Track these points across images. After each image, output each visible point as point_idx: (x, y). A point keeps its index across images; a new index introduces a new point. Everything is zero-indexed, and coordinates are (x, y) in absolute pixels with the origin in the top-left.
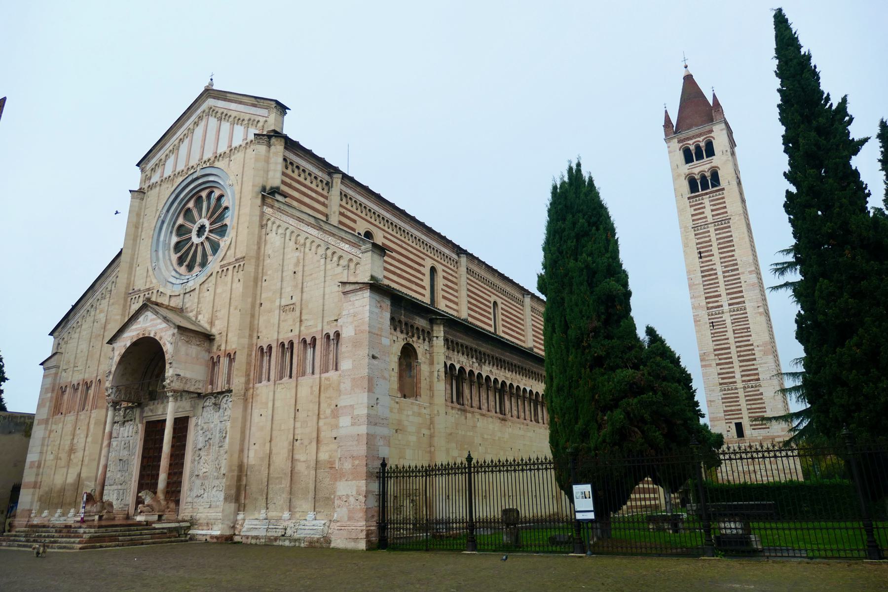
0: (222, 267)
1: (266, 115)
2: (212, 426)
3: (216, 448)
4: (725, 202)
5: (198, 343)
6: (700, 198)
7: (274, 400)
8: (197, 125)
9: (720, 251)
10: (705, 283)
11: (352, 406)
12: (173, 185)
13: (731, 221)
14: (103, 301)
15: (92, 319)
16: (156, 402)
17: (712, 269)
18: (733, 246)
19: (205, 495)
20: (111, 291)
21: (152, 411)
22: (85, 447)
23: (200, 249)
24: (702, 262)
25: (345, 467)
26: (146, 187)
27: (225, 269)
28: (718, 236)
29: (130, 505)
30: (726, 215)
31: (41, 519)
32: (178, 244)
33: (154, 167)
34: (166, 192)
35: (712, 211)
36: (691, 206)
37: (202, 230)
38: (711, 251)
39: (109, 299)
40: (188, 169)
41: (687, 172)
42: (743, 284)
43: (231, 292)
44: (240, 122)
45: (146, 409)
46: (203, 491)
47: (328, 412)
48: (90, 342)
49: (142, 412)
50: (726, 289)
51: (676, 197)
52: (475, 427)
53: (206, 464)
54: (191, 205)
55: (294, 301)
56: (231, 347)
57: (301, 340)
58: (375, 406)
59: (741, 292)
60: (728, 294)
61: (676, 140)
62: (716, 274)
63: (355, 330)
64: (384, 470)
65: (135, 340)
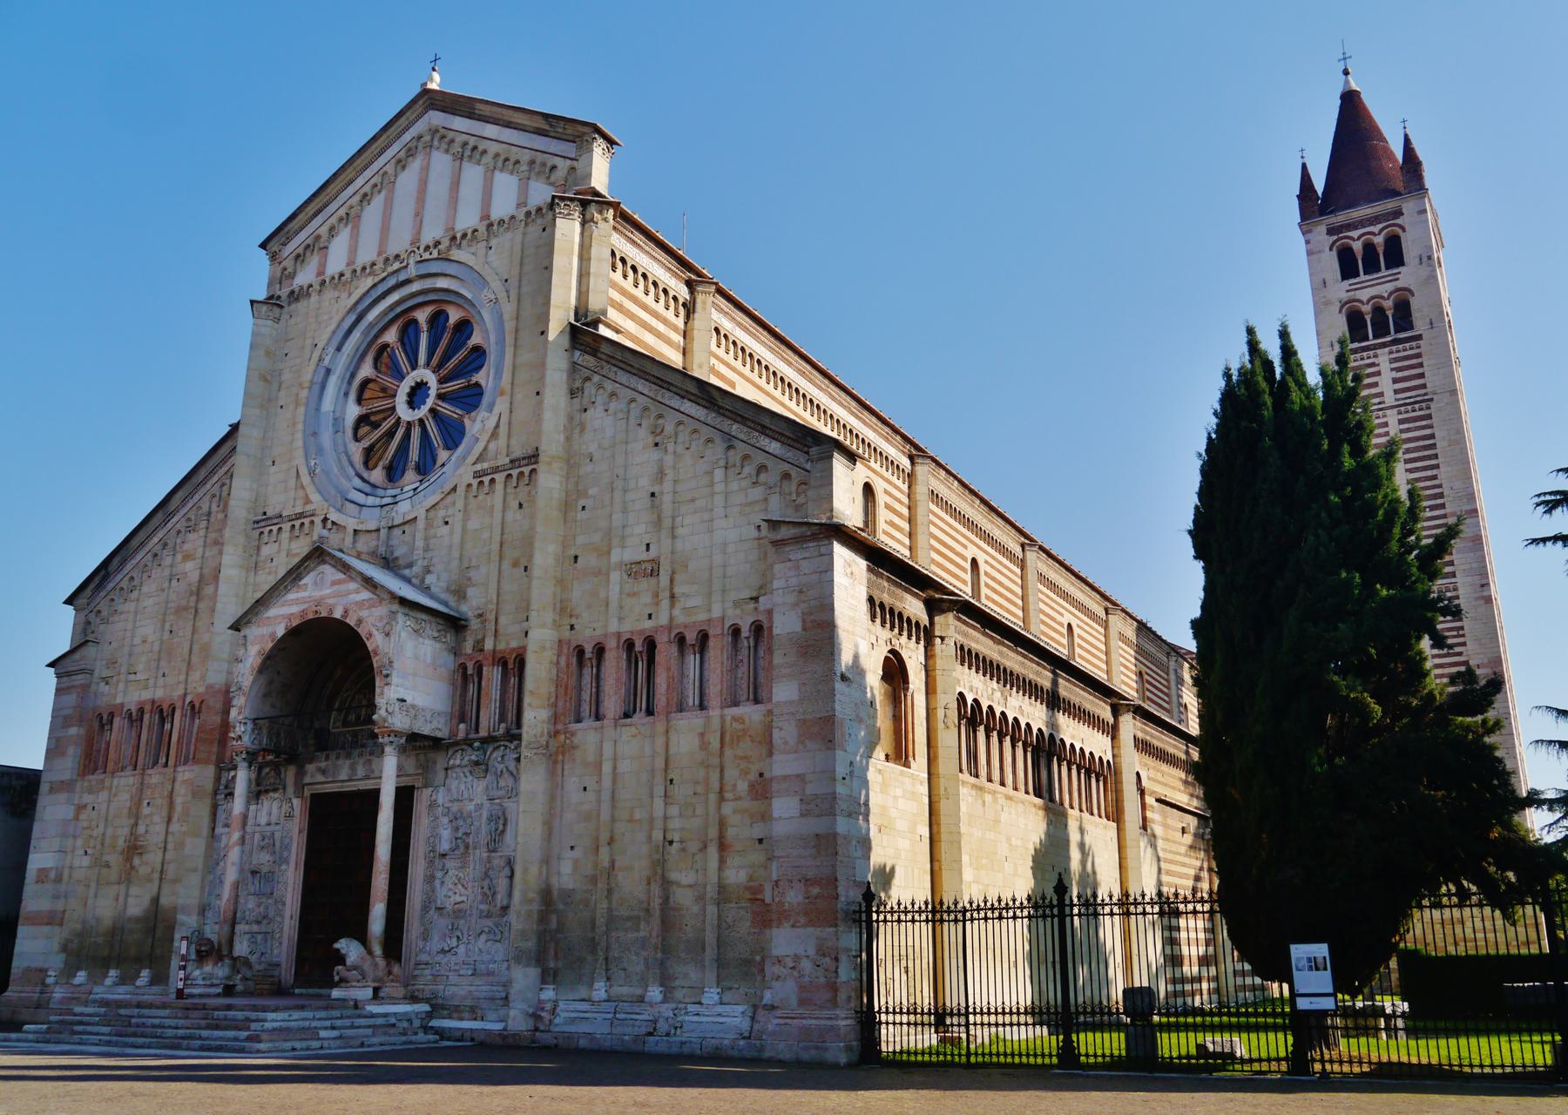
0: (477, 475)
1: (573, 156)
2: (471, 807)
3: (482, 853)
4: (1421, 365)
5: (436, 634)
6: (1371, 353)
7: (615, 760)
8: (404, 167)
11: (800, 777)
12: (350, 294)
13: (1433, 405)
14: (191, 536)
15: (167, 572)
16: (333, 755)
18: (1436, 456)
19: (462, 949)
20: (209, 513)
21: (324, 772)
22: (166, 842)
23: (416, 433)
25: (788, 899)
26: (284, 293)
27: (486, 479)
29: (283, 966)
30: (1423, 391)
31: (72, 990)
32: (362, 420)
33: (300, 250)
34: (332, 309)
35: (1395, 381)
37: (418, 392)
39: (207, 532)
40: (387, 259)
41: (1345, 296)
43: (502, 529)
44: (510, 165)
45: (310, 768)
46: (455, 940)
47: (743, 786)
48: (164, 621)
49: (301, 773)
51: (1319, 348)
52: (997, 822)
53: (460, 886)
54: (391, 336)
56: (508, 643)
57: (673, 635)
58: (848, 778)
61: (1323, 229)
63: (804, 621)
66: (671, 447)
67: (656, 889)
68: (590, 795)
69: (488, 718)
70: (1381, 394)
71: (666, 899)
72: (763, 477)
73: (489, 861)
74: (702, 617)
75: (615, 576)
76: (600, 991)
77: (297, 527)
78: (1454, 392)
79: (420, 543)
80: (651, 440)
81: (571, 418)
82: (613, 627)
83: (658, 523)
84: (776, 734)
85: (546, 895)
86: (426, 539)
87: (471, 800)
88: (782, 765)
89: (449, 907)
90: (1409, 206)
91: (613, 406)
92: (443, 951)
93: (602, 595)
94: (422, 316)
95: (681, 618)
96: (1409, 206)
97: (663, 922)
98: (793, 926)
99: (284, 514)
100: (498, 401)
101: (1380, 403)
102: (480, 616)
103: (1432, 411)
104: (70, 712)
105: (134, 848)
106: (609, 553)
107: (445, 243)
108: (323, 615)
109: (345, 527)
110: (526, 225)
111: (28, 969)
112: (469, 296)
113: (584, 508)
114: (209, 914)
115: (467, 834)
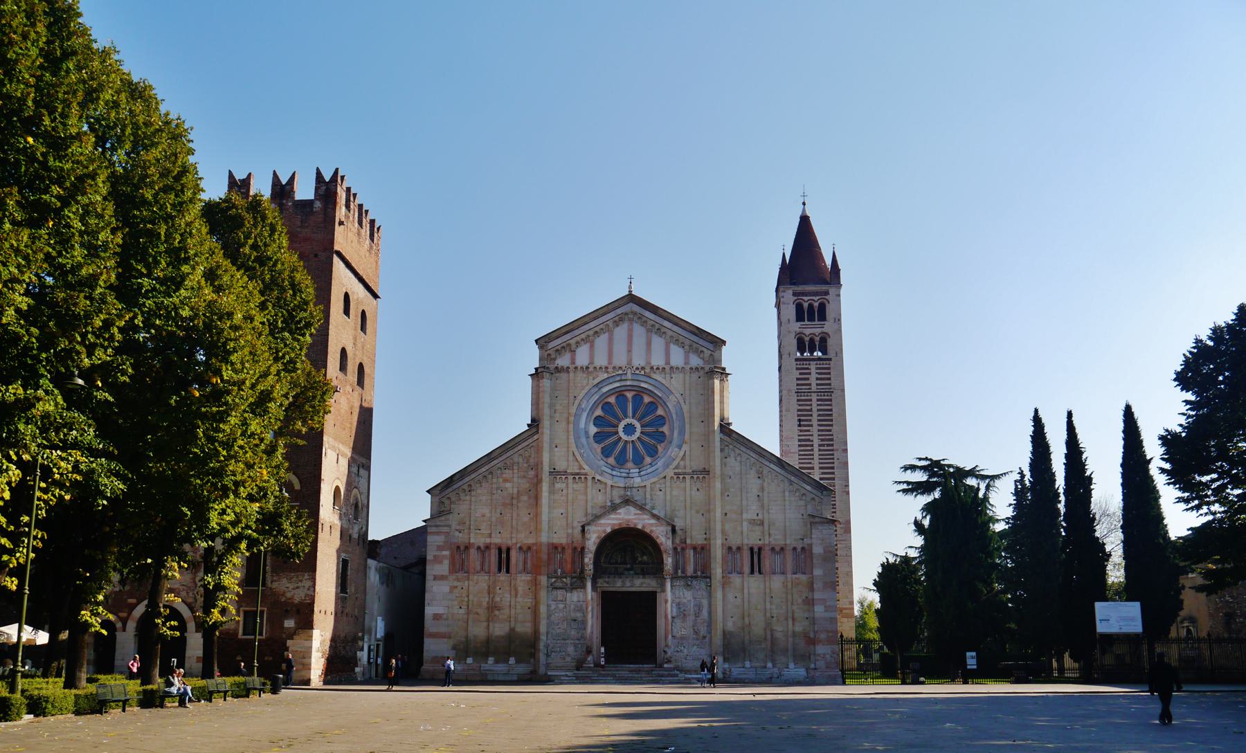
0: (675, 474)
3: (692, 618)
4: (829, 374)
6: (808, 362)
8: (617, 326)
9: (819, 423)
10: (801, 453)
11: (824, 600)
14: (507, 471)
17: (809, 440)
18: (832, 420)
19: (685, 651)
20: (518, 463)
21: (608, 583)
24: (801, 431)
26: (552, 367)
28: (819, 408)
35: (817, 379)
36: (797, 369)
38: (810, 420)
41: (798, 330)
42: (835, 461)
47: (800, 601)
50: (820, 463)
55: (760, 517)
59: (833, 468)
60: (821, 468)
61: (790, 292)
62: (812, 445)
63: (824, 550)
64: (842, 639)
65: (616, 528)
66: (766, 480)
67: (769, 633)
68: (739, 601)
69: (690, 570)
70: (810, 385)
71: (772, 635)
72: (804, 498)
73: (696, 620)
74: (783, 543)
75: (745, 524)
76: (748, 664)
77: (583, 479)
79: (648, 496)
80: (757, 475)
81: (721, 460)
82: (746, 541)
83: (762, 506)
84: (815, 586)
85: (724, 633)
86: (651, 495)
88: (817, 595)
89: (678, 636)
91: (739, 458)
92: (678, 651)
93: (739, 529)
94: (629, 395)
95: (773, 542)
96: (832, 291)
97: (772, 641)
98: (823, 645)
101: (809, 389)
102: (681, 530)
104: (442, 544)
105: (493, 607)
106: (742, 514)
107: (648, 370)
108: (632, 526)
109: (606, 484)
110: (690, 373)
111: (436, 657)
112: (660, 395)
114: (550, 636)
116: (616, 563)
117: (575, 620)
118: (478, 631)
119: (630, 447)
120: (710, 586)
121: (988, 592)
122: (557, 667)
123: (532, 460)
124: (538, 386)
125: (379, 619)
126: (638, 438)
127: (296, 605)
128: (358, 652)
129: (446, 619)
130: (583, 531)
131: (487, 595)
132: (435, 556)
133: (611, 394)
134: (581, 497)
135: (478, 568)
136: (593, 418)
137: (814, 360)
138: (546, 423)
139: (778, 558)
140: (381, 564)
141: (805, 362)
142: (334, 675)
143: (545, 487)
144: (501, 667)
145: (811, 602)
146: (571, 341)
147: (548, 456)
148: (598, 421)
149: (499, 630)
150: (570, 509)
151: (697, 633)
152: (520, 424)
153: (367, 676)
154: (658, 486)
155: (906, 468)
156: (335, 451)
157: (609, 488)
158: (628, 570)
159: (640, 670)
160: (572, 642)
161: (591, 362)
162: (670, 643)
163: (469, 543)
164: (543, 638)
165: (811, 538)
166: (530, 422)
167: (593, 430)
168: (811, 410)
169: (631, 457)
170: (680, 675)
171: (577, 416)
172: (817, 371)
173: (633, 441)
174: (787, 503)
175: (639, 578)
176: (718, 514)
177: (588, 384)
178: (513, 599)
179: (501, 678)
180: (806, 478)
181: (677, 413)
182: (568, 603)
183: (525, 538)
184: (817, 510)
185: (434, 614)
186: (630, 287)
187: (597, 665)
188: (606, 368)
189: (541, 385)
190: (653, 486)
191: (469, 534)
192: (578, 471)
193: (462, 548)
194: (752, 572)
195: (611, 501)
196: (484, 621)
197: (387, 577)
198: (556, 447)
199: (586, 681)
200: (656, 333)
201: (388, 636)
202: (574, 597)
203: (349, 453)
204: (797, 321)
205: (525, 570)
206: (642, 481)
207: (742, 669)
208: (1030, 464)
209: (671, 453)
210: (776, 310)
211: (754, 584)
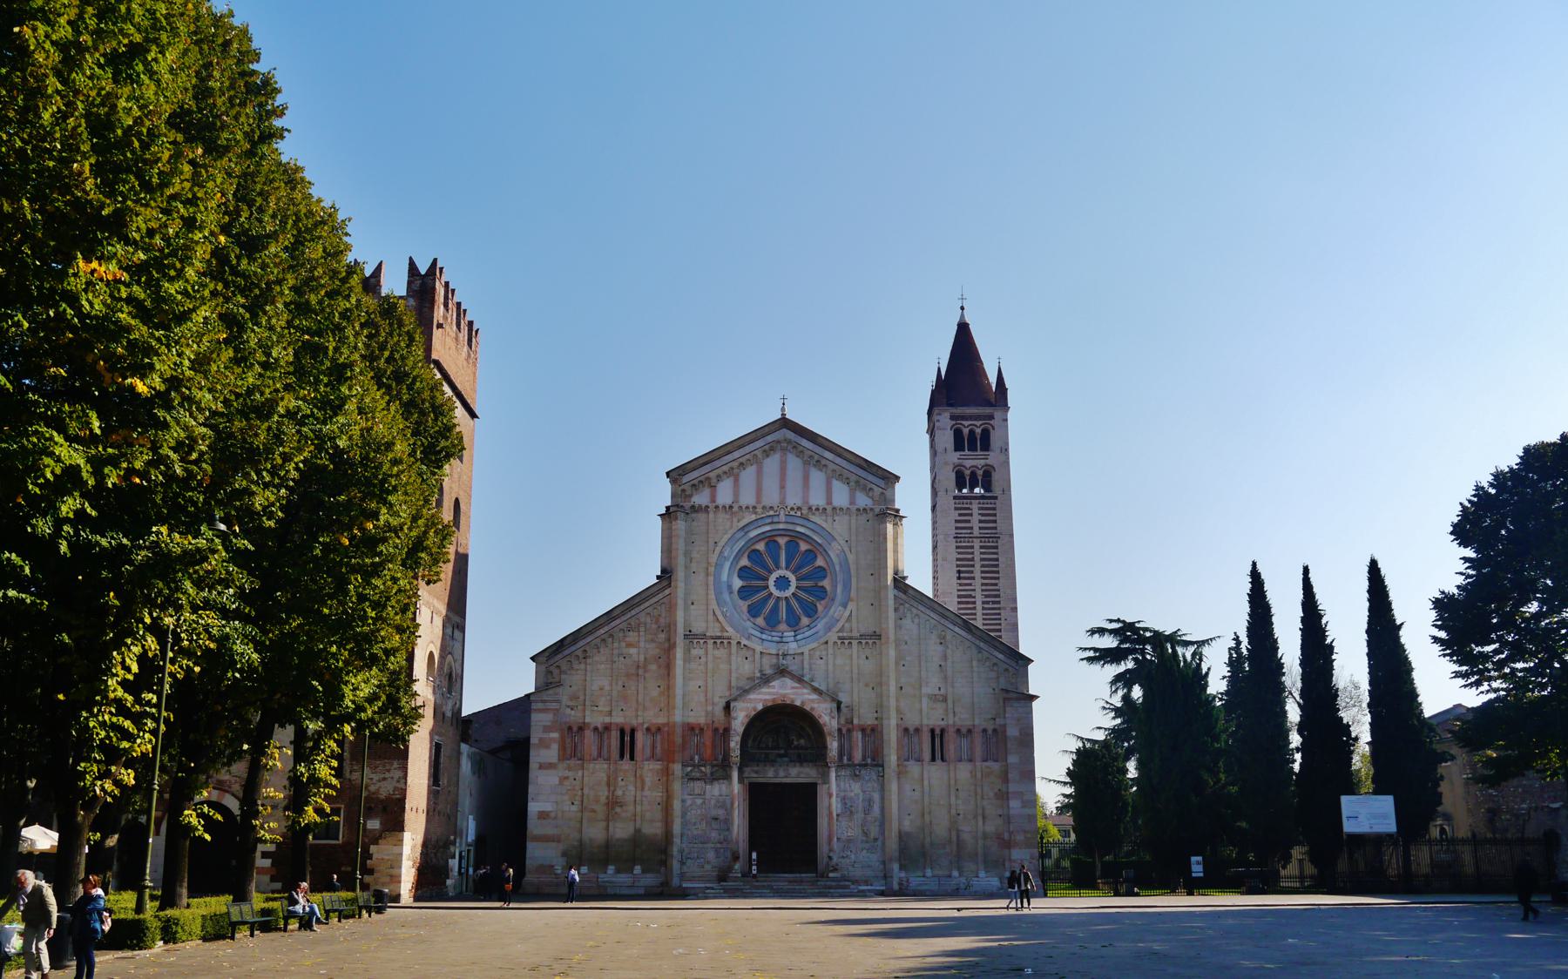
0: (839, 638)
3: (859, 816)
8: (768, 456)
9: (983, 575)
11: (1022, 792)
14: (631, 633)
17: (970, 596)
18: (998, 572)
19: (853, 856)
20: (645, 624)
21: (756, 772)
24: (960, 585)
26: (687, 505)
27: (847, 642)
30: (994, 531)
35: (980, 521)
36: (956, 509)
38: (972, 572)
41: (956, 461)
45: (747, 770)
47: (991, 794)
55: (942, 691)
61: (947, 415)
62: (974, 603)
64: (1042, 841)
65: (770, 704)
66: (950, 646)
69: (858, 756)
70: (971, 528)
71: (958, 837)
72: (995, 668)
73: (865, 818)
74: (971, 723)
75: (925, 700)
76: (929, 873)
78: (1012, 536)
79: (806, 666)
80: (938, 641)
82: (925, 722)
83: (945, 678)
84: (1010, 776)
85: (902, 836)
86: (810, 664)
87: (852, 791)
88: (1012, 788)
90: (998, 414)
91: (916, 620)
92: (843, 857)
94: (782, 541)
95: (959, 723)
96: (998, 414)
97: (958, 844)
98: (1020, 848)
99: (708, 634)
100: (850, 603)
102: (847, 707)
103: (999, 544)
104: (549, 724)
105: (613, 803)
109: (754, 650)
111: (541, 866)
112: (819, 541)
113: (904, 665)
114: (685, 838)
115: (851, 806)
116: (767, 748)
117: (717, 819)
118: (595, 833)
119: (783, 604)
120: (883, 776)
121: (1215, 783)
122: (694, 877)
123: (662, 620)
124: (670, 529)
125: (471, 817)
126: (793, 594)
127: (382, 801)
128: (450, 860)
129: (555, 818)
130: (727, 707)
131: (606, 788)
132: (541, 739)
133: (763, 539)
134: (723, 666)
135: (595, 754)
136: (739, 567)
137: (976, 498)
138: (680, 574)
139: (964, 743)
140: (473, 749)
141: (965, 501)
142: (425, 889)
143: (679, 653)
144: (623, 878)
145: (1005, 796)
146: (711, 475)
147: (683, 615)
148: (743, 574)
149: (622, 831)
150: (709, 680)
151: (866, 834)
152: (648, 575)
153: (458, 890)
154: (818, 653)
155: (1093, 632)
156: (429, 608)
157: (757, 656)
158: (780, 756)
159: (802, 882)
160: (713, 845)
161: (736, 501)
162: (835, 847)
163: (584, 723)
164: (677, 840)
165: (1005, 717)
166: (659, 574)
167: (738, 583)
168: (972, 559)
169: (784, 617)
170: (852, 886)
171: (719, 566)
172: (980, 512)
173: (786, 597)
174: (975, 674)
175: (795, 766)
176: (893, 688)
177: (731, 527)
178: (638, 793)
179: (625, 892)
180: (998, 645)
181: (840, 564)
182: (707, 796)
183: (653, 717)
184: (1012, 684)
185: (539, 812)
186: (783, 409)
187: (746, 874)
188: (754, 507)
189: (673, 527)
190: (812, 652)
191: (584, 710)
192: (719, 634)
193: (575, 729)
194: (933, 759)
195: (761, 671)
196: (602, 820)
197: (479, 766)
198: (693, 604)
199: (737, 894)
200: (815, 466)
201: (480, 839)
202: (715, 790)
203: (443, 609)
204: (956, 450)
205: (653, 757)
206: (799, 647)
207: (923, 879)
208: (1248, 628)
209: (834, 613)
210: (928, 436)
211: (935, 774)
